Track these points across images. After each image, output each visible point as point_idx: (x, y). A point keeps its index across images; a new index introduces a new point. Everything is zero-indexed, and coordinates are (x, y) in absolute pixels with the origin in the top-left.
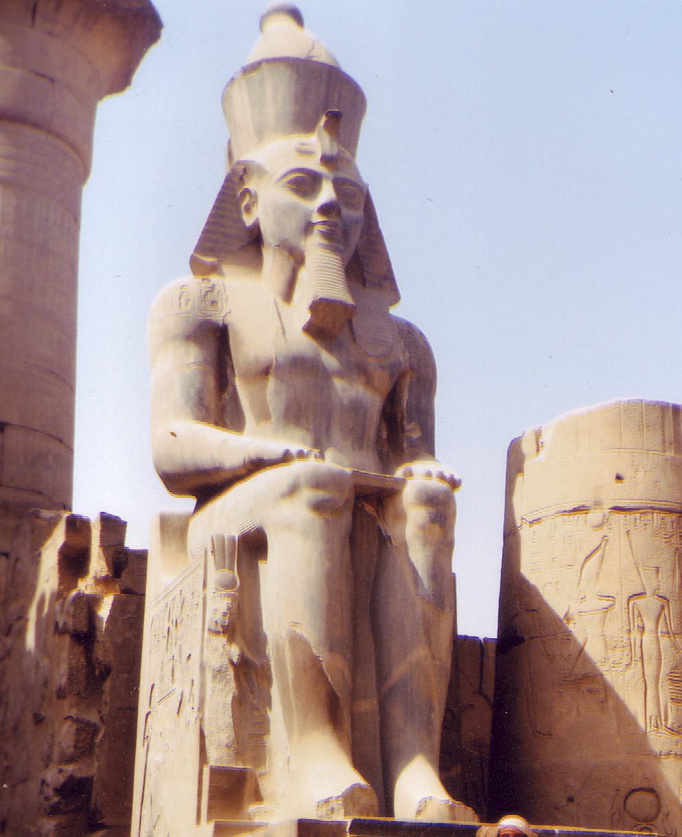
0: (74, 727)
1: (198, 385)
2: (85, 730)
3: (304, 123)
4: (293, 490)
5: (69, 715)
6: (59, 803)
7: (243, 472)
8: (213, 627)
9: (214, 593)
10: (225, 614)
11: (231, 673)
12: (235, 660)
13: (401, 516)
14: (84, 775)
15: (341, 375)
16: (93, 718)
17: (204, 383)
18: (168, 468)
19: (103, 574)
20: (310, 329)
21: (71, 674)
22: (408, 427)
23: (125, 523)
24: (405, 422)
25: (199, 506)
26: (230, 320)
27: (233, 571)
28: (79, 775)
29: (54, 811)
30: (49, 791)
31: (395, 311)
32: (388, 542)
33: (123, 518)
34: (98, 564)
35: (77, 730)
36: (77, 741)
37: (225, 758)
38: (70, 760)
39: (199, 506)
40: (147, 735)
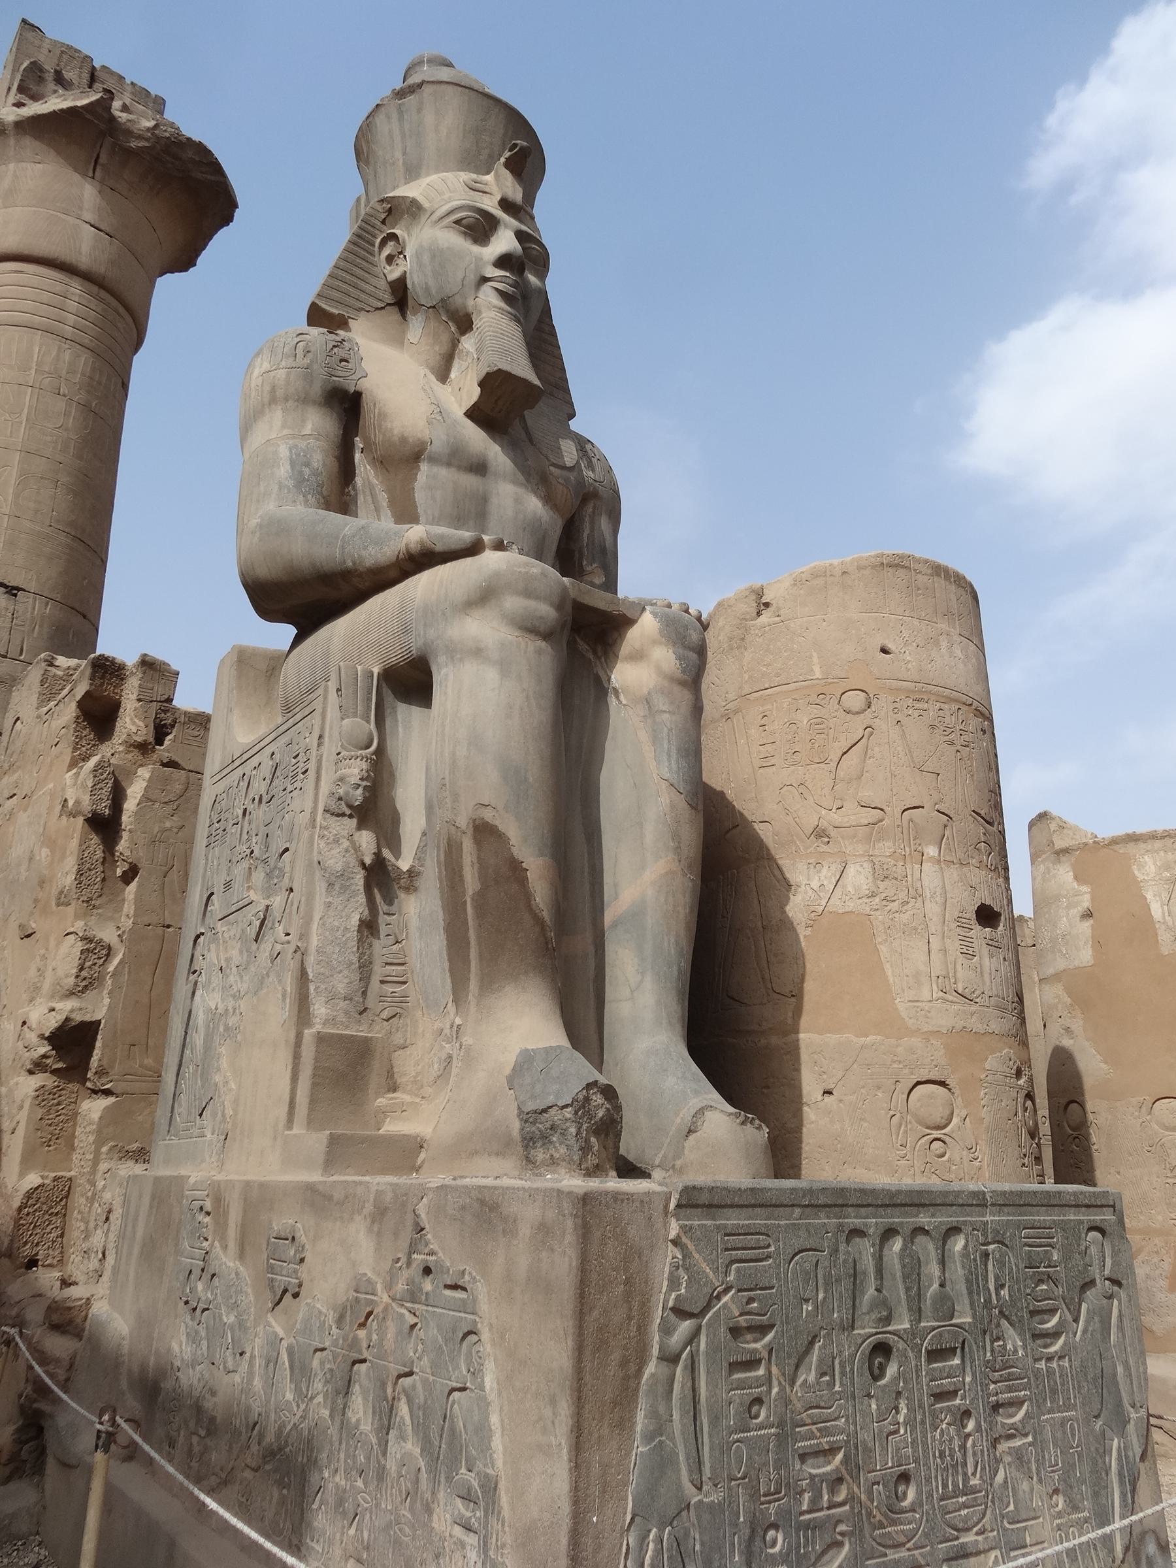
0: (80, 946)
2: (95, 951)
5: (72, 930)
8: (333, 806)
9: (339, 754)
11: (359, 878)
12: (368, 861)
14: (88, 1018)
16: (108, 935)
18: (262, 572)
19: (139, 739)
21: (80, 873)
22: (589, 569)
24: (585, 563)
27: (368, 722)
28: (78, 1018)
29: (38, 1066)
30: (32, 1037)
34: (131, 722)
35: (82, 952)
36: (81, 969)
37: (341, 1018)
38: (71, 994)
40: (196, 967)
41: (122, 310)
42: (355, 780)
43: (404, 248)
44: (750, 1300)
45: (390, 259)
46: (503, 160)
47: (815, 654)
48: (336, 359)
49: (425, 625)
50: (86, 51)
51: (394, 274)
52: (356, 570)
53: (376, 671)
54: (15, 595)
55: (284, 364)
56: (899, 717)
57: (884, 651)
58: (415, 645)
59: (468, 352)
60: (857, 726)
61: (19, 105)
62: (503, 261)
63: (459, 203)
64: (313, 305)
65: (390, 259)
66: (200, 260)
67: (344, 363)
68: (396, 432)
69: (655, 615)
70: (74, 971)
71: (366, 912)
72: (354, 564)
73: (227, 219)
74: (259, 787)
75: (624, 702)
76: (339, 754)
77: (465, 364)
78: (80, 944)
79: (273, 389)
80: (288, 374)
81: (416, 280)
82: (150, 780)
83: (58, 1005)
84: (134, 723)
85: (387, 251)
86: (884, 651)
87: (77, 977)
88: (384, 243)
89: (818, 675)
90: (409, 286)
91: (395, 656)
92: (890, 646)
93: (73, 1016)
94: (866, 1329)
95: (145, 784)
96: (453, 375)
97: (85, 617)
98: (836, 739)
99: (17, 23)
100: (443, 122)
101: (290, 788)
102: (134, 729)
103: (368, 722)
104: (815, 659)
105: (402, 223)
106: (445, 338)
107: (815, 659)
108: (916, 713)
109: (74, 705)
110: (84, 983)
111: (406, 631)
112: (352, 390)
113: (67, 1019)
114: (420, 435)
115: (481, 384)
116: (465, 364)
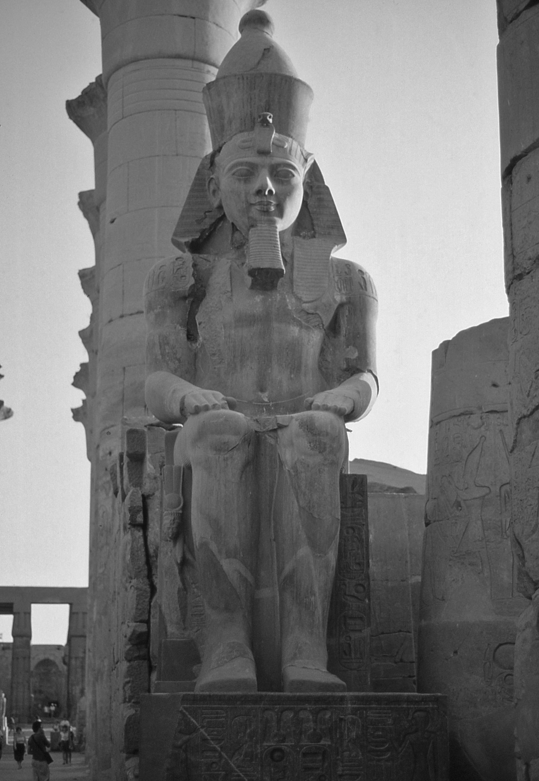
6: (130, 650)
11: (177, 570)
31: (339, 253)
35: (137, 596)
42: (168, 526)
44: (212, 731)
45: (214, 191)
53: (182, 465)
67: (184, 278)
70: (135, 606)
71: (181, 585)
78: (136, 591)
83: (130, 624)
85: (212, 187)
87: (137, 608)
93: (137, 629)
94: (271, 744)
110: (140, 612)
113: (134, 631)
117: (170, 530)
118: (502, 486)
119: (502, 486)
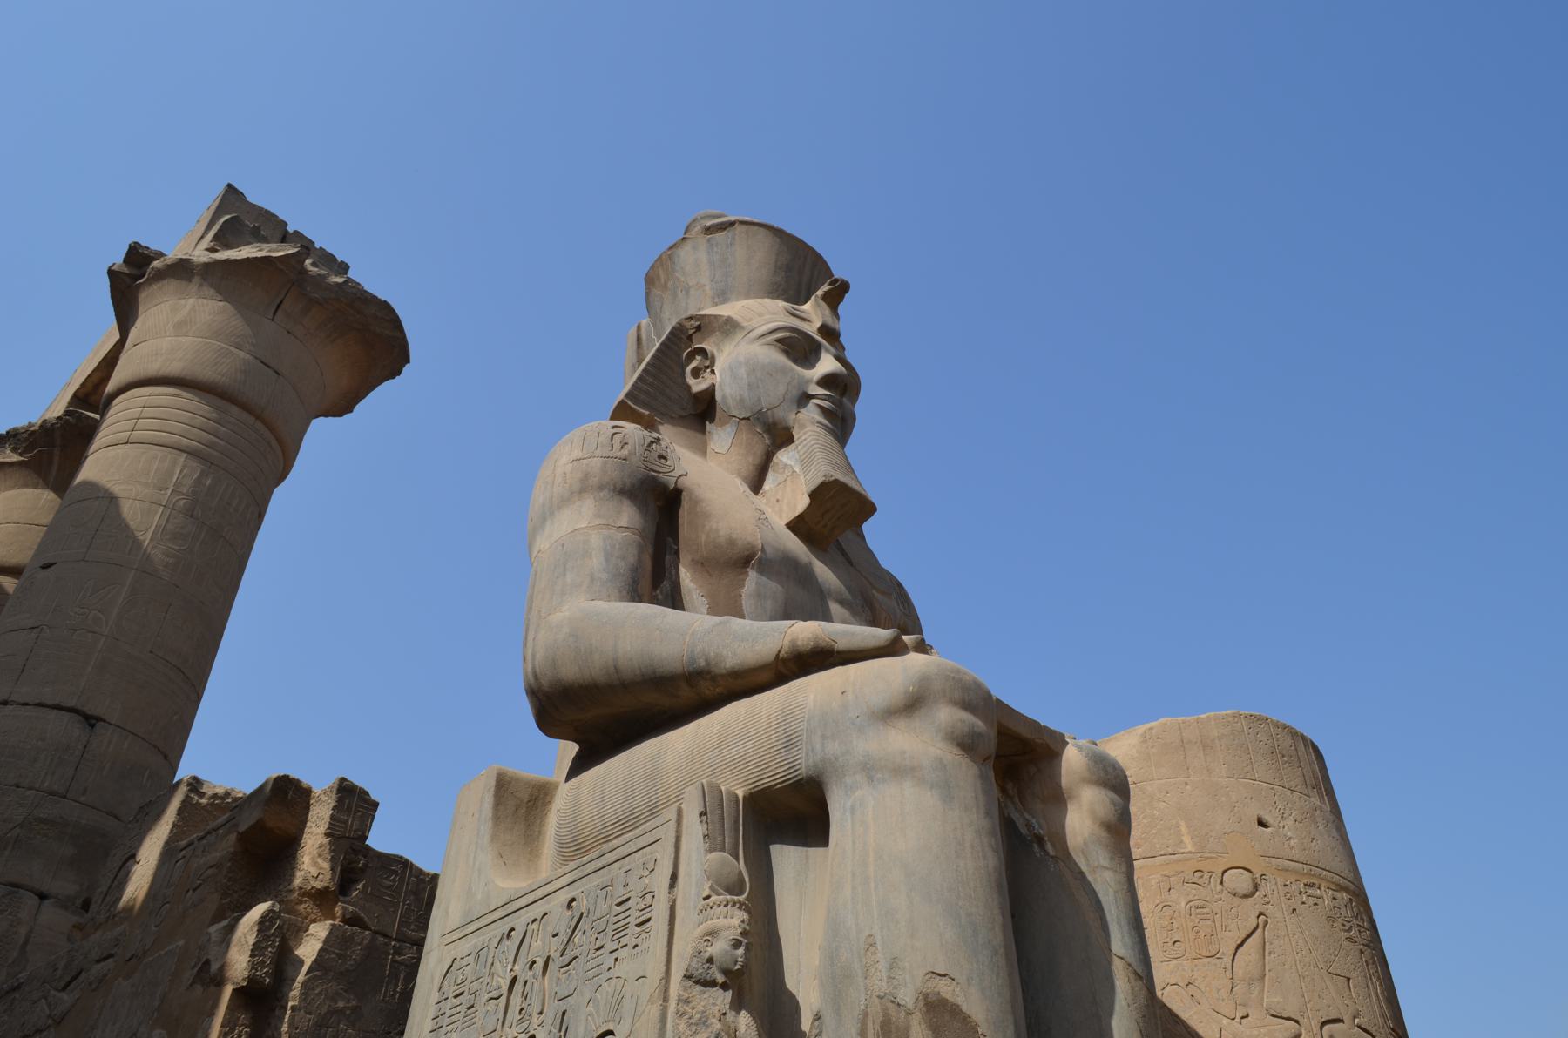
1: (632, 560)
3: (776, 292)
4: (912, 704)
7: (765, 677)
8: (699, 970)
9: (708, 897)
10: (736, 944)
13: (1059, 799)
15: (842, 602)
17: (640, 560)
19: (318, 885)
20: (795, 526)
23: (375, 805)
25: (579, 766)
26: (684, 482)
27: (737, 859)
32: (1036, 848)
33: (374, 796)
39: (579, 766)
41: (274, 443)
42: (735, 933)
43: (713, 363)
46: (820, 293)
47: (1182, 823)
48: (654, 455)
49: (824, 737)
50: (282, 216)
51: (697, 386)
52: (709, 672)
53: (740, 793)
54: (92, 726)
55: (598, 453)
56: (1296, 903)
57: (1262, 823)
58: (804, 763)
59: (786, 465)
60: (1248, 911)
61: (212, 250)
62: (827, 381)
63: (781, 324)
64: (622, 403)
65: (696, 373)
66: (358, 408)
68: (722, 533)
69: (1080, 748)
72: (708, 663)
73: (395, 373)
74: (538, 947)
75: (1052, 853)
76: (708, 897)
77: (781, 478)
79: (586, 476)
80: (605, 464)
81: (728, 391)
82: (326, 942)
84: (315, 864)
86: (1262, 823)
88: (691, 357)
89: (1190, 848)
90: (718, 397)
91: (773, 773)
92: (1267, 818)
95: (319, 945)
96: (767, 486)
97: (166, 757)
98: (1225, 928)
99: (221, 188)
100: (751, 257)
101: (611, 946)
102: (314, 872)
103: (737, 859)
104: (1183, 829)
105: (713, 339)
106: (760, 449)
107: (1183, 829)
108: (1311, 901)
109: (233, 837)
111: (789, 745)
112: (672, 486)
114: (750, 539)
115: (814, 495)
116: (781, 478)
117: (741, 951)
118: (1324, 1024)
119: (1324, 1024)
